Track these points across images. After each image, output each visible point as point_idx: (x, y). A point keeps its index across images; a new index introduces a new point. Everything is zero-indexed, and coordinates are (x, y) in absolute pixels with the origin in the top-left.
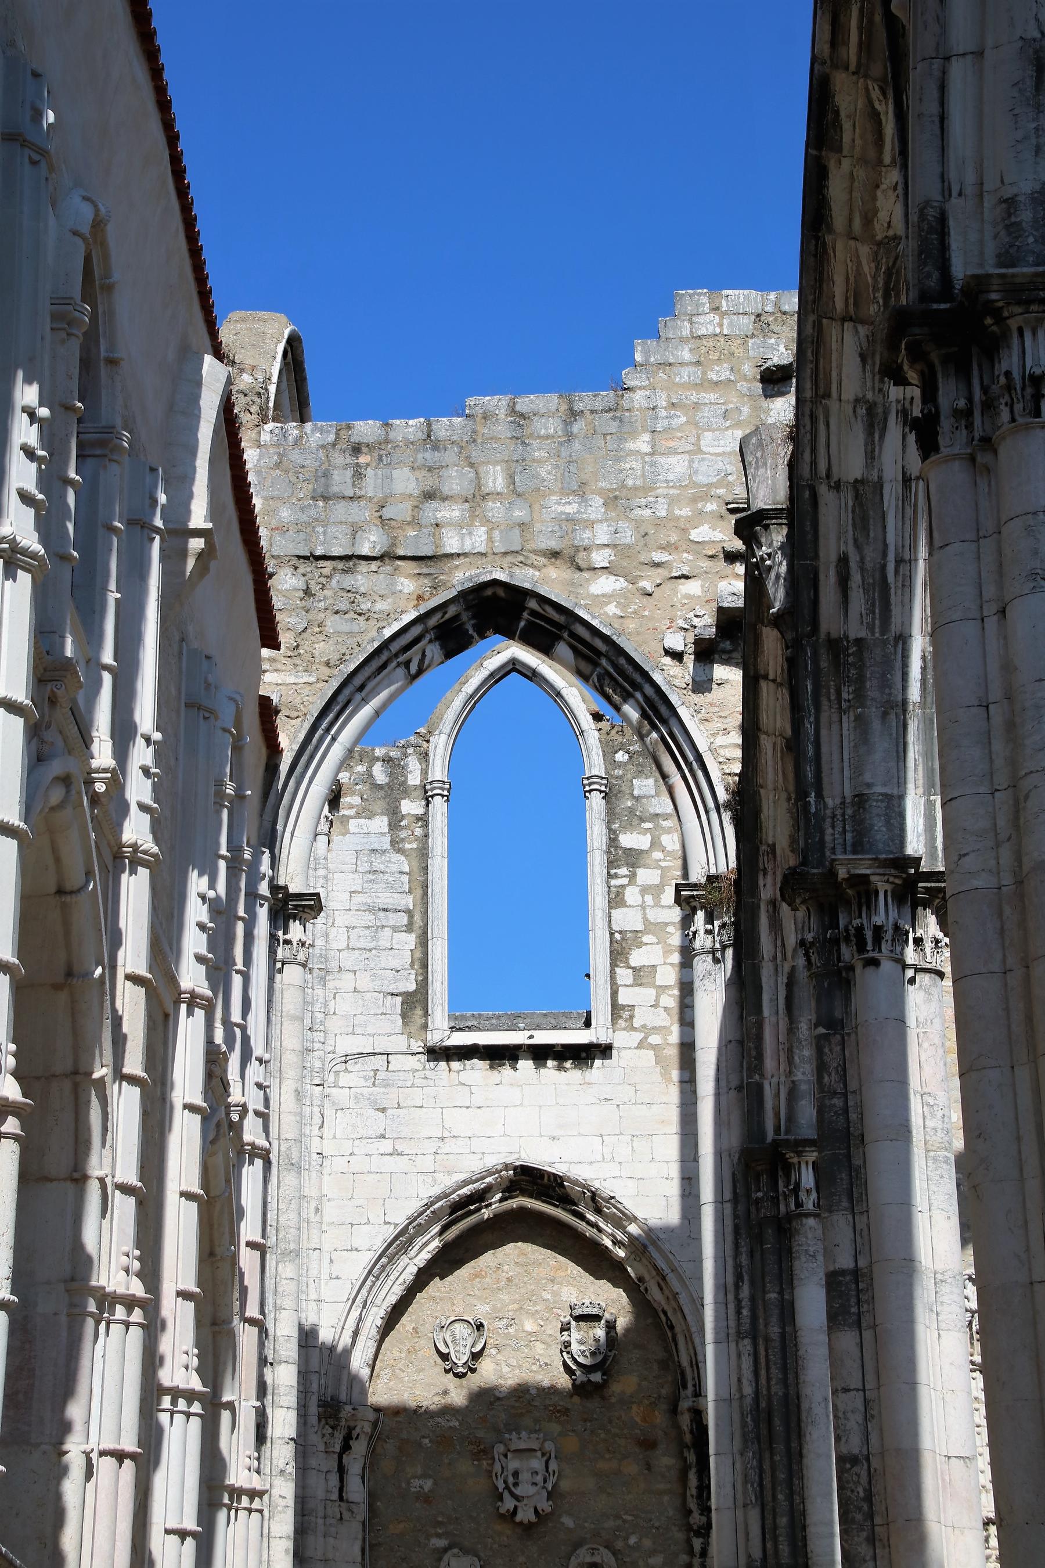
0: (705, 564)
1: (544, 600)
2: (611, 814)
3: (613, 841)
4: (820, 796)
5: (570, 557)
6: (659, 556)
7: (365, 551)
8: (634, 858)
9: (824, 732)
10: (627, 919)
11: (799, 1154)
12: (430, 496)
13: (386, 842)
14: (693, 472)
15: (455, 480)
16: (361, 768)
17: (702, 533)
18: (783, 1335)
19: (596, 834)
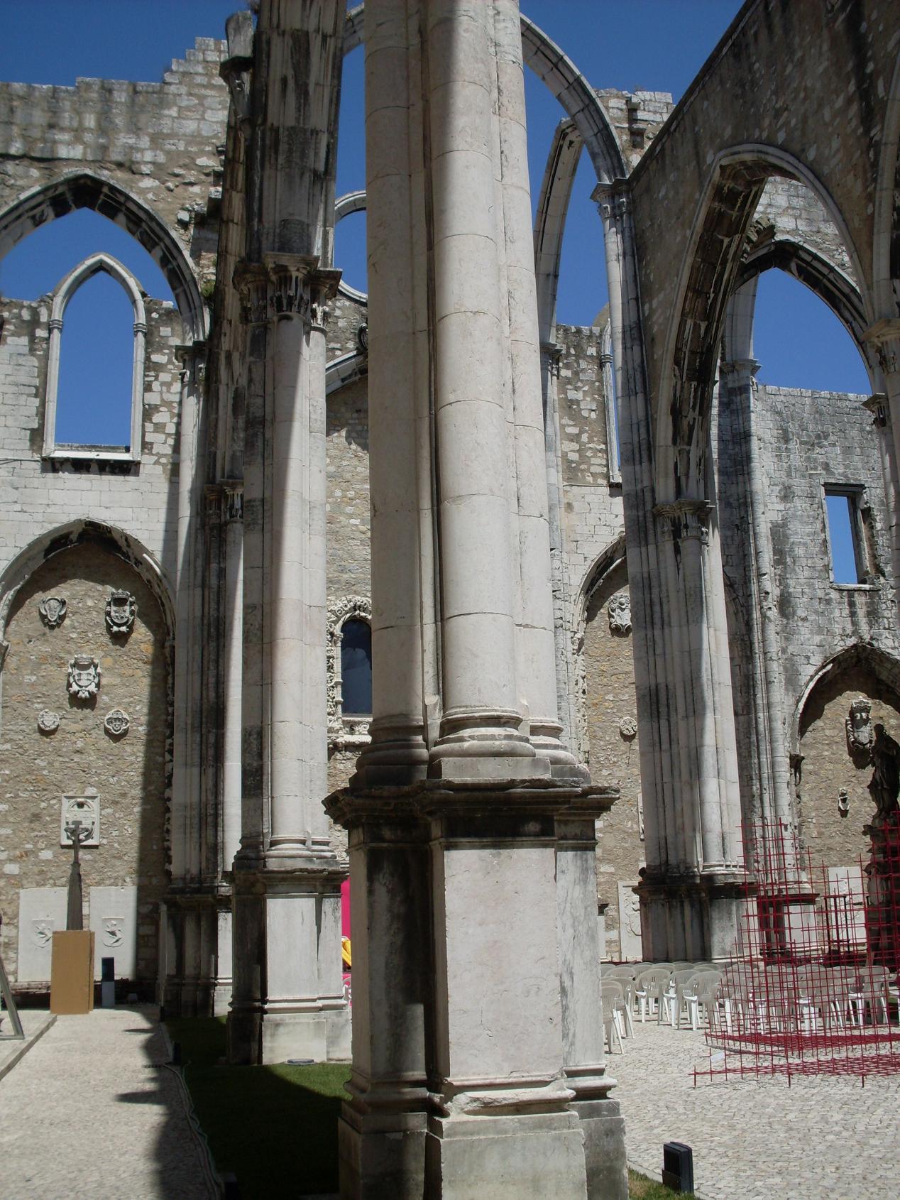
0: (203, 177)
1: (112, 188)
2: (148, 344)
3: (148, 359)
4: (260, 221)
5: (129, 167)
6: (178, 171)
7: (13, 151)
8: (158, 368)
9: (266, 184)
10: (153, 398)
11: (234, 489)
12: (51, 126)
13: (26, 350)
14: (199, 130)
15: (66, 118)
16: (15, 311)
17: (202, 161)
18: (219, 587)
19: (140, 354)
